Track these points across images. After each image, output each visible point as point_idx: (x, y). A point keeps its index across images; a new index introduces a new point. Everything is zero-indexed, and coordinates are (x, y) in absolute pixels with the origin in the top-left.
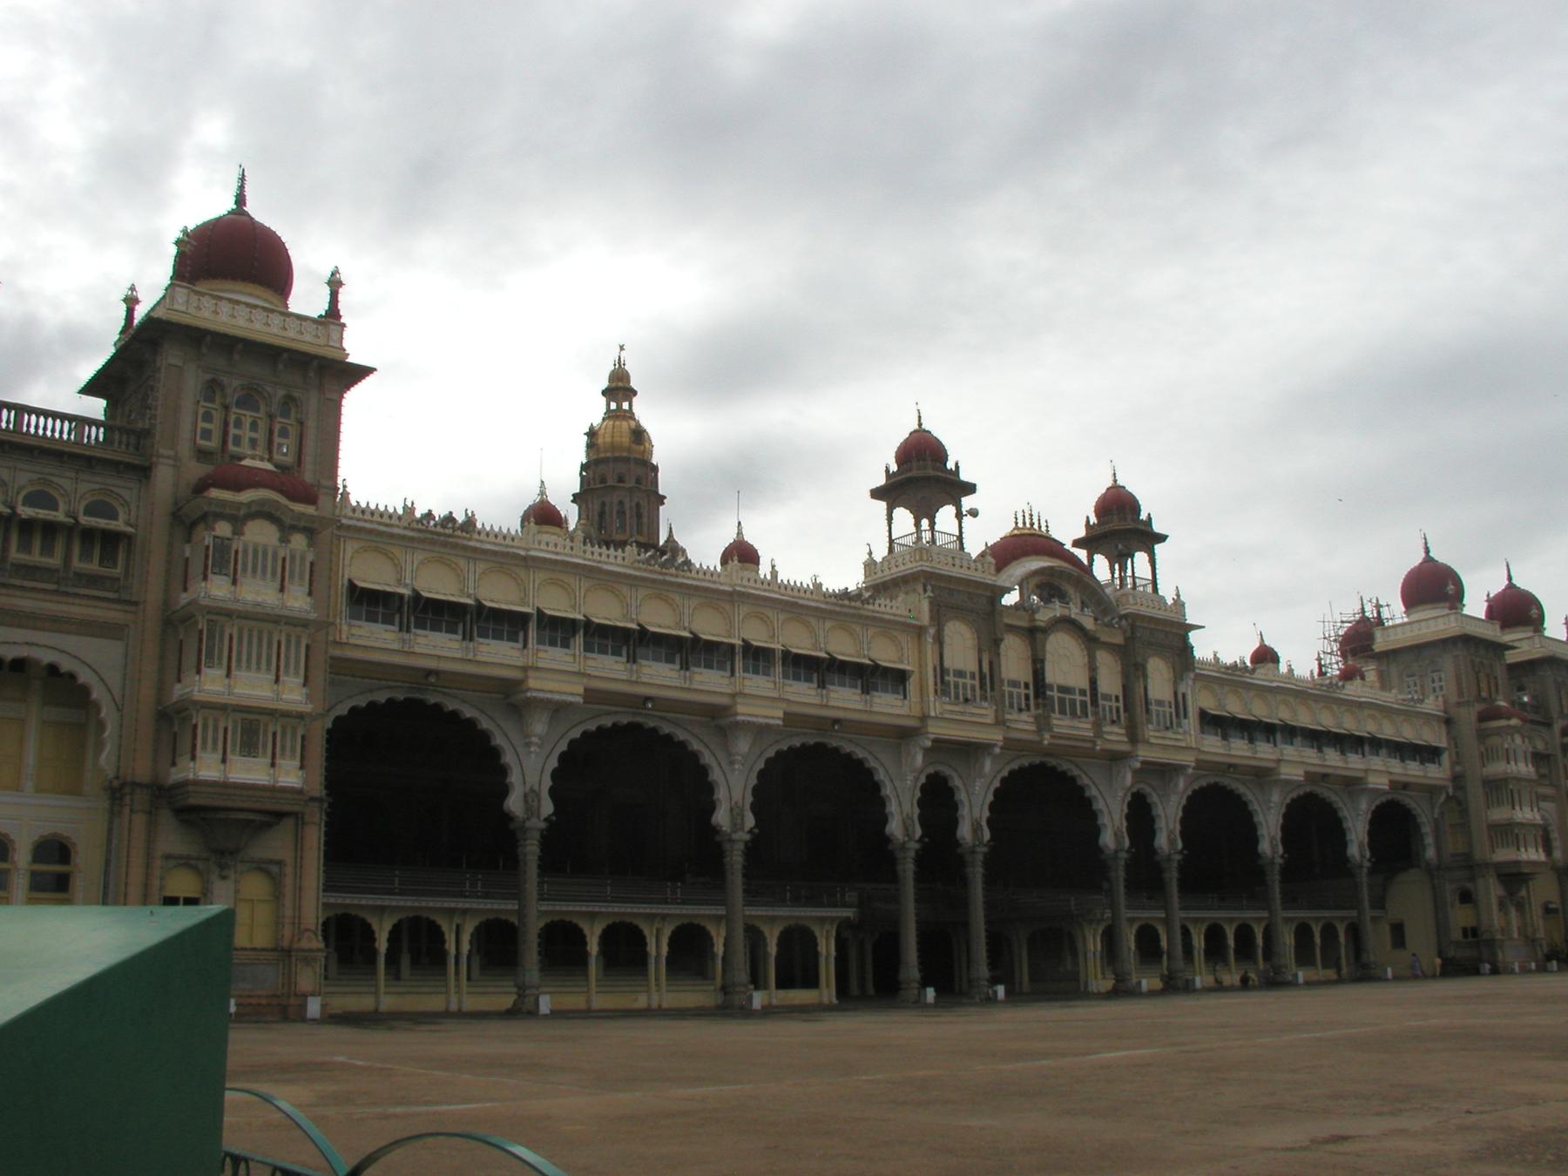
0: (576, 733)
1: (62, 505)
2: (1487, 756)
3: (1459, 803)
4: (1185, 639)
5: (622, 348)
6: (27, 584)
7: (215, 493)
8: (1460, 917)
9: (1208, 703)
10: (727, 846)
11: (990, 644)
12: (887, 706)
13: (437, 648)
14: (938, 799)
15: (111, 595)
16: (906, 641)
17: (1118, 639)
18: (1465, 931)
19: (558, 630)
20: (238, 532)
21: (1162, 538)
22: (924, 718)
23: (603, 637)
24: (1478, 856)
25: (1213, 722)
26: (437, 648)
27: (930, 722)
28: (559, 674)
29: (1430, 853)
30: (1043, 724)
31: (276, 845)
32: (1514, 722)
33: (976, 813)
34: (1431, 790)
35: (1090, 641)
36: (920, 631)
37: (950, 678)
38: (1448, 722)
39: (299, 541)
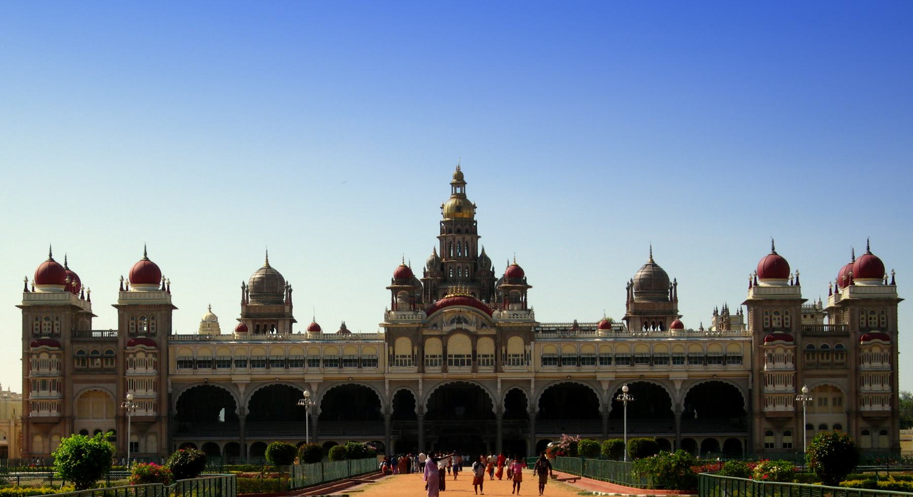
0: (257, 390)
9: (551, 350)
12: (368, 372)
13: (204, 374)
14: (404, 398)
17: (493, 331)
20: (135, 356)
21: (531, 287)
23: (256, 363)
26: (204, 374)
28: (241, 376)
29: (745, 407)
30: (445, 370)
31: (155, 428)
33: (421, 403)
35: (474, 337)
37: (399, 359)
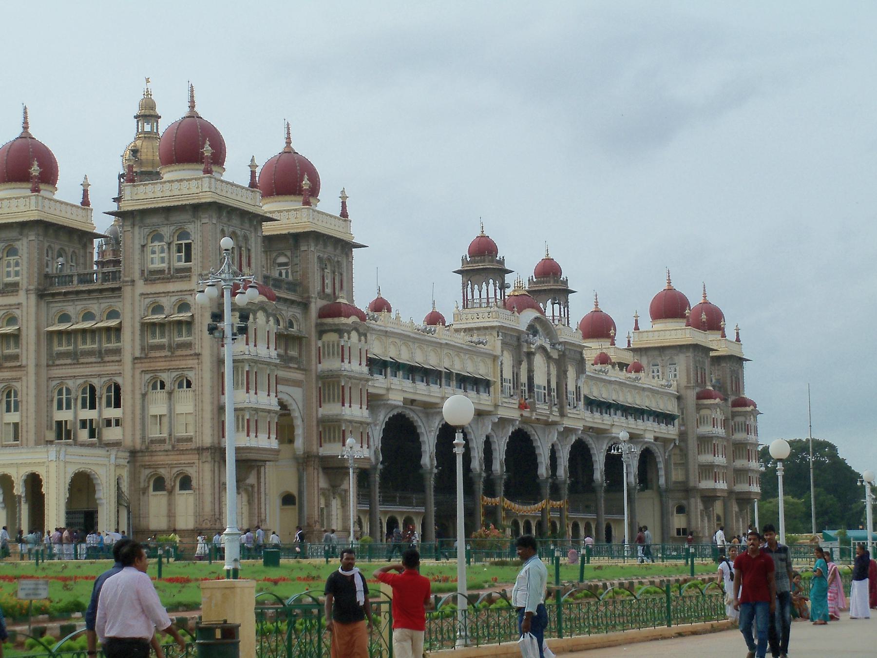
1: (295, 326)
2: (701, 421)
3: (681, 450)
4: (581, 353)
5: (148, 81)
6: (291, 365)
7: (343, 320)
8: (678, 522)
10: (428, 476)
11: (518, 363)
15: (296, 366)
16: (489, 362)
17: (555, 356)
18: (678, 530)
19: (397, 367)
22: (496, 406)
24: (692, 484)
25: (593, 404)
27: (500, 408)
29: (662, 481)
32: (718, 400)
34: (665, 441)
35: (548, 357)
36: (495, 358)
38: (679, 398)
39: (363, 338)
